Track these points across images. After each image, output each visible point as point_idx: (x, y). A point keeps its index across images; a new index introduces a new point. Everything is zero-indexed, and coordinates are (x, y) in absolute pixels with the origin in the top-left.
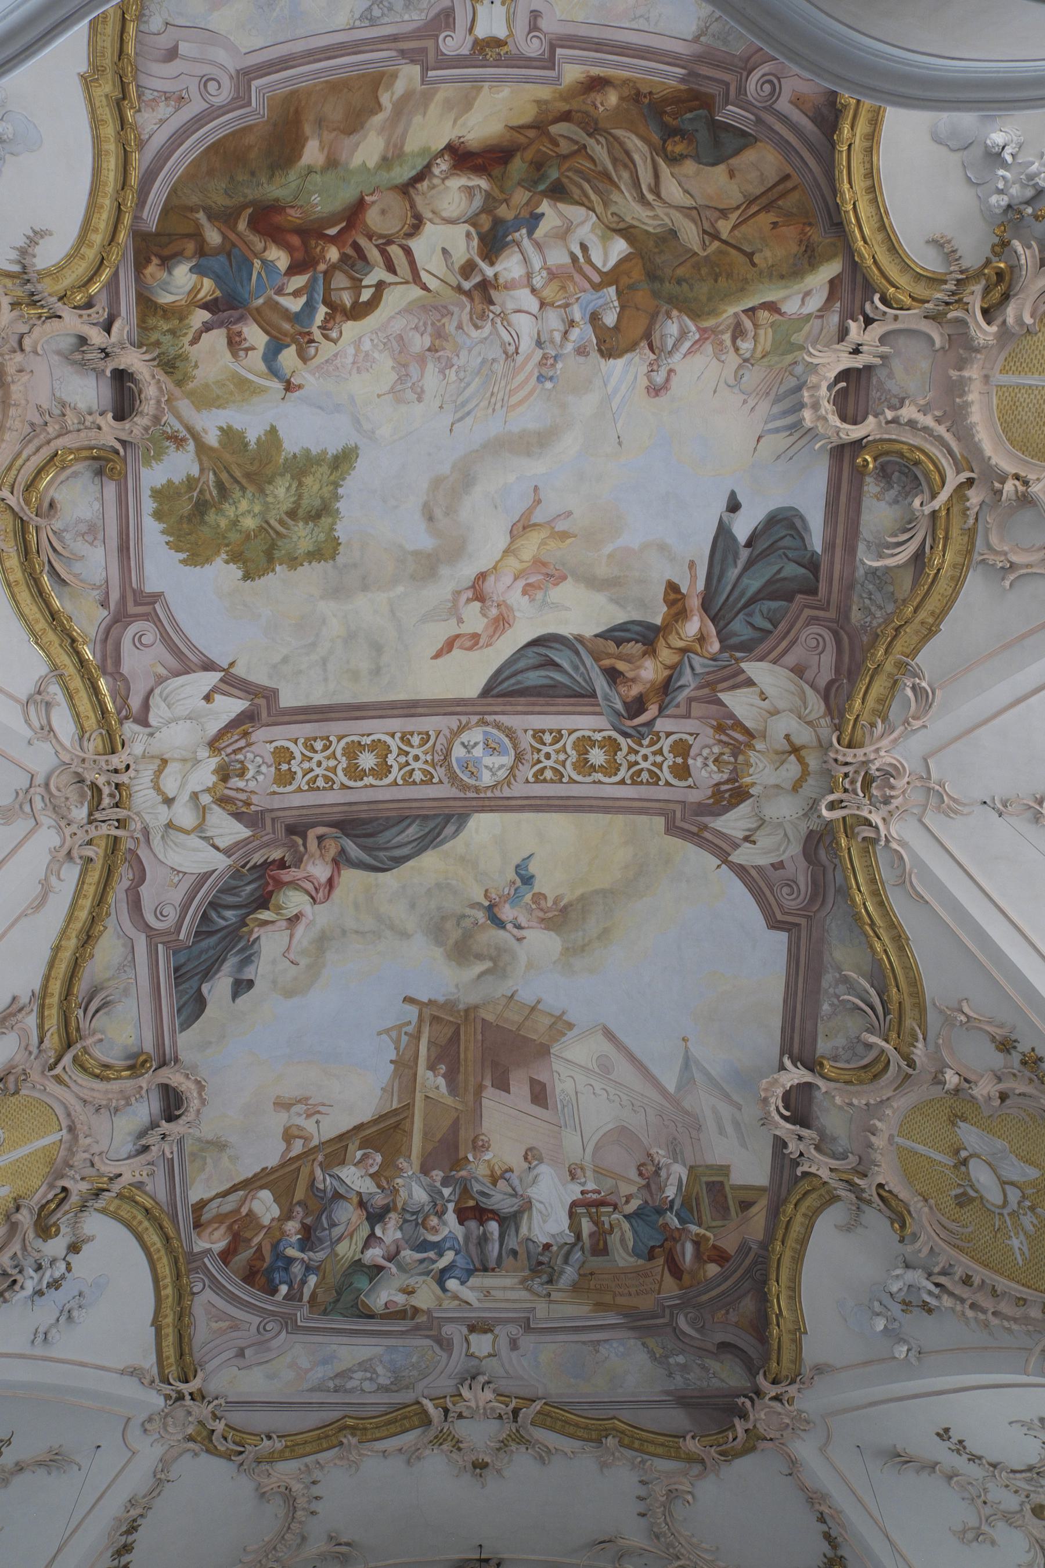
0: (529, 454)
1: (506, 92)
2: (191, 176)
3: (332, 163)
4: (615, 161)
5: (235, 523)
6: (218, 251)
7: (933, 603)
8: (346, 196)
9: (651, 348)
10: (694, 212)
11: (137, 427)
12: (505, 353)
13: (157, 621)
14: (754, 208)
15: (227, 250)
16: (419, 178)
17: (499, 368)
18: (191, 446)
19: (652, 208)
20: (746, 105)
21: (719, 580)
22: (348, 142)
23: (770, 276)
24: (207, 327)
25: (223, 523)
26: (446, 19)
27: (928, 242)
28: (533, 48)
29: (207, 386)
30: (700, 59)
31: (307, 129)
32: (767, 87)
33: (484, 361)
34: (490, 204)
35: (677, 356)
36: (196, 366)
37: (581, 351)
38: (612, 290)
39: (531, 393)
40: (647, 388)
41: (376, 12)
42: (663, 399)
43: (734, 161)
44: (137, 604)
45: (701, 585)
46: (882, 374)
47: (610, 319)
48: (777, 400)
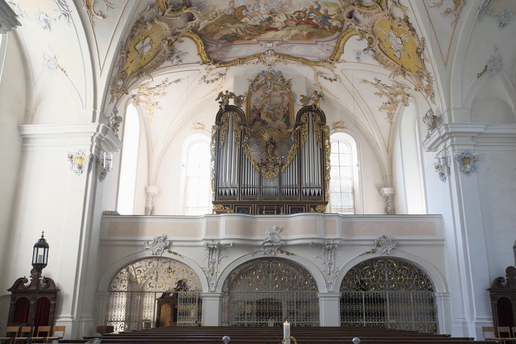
1: (267, 37)
2: (328, 36)
4: (245, 31)
6: (326, 25)
8: (299, 27)
9: (234, 8)
10: (228, 28)
11: (351, 8)
12: (267, 5)
14: (217, 32)
15: (324, 24)
16: (284, 27)
17: (268, 2)
19: (238, 27)
22: (298, 33)
23: (211, 24)
24: (331, 15)
26: (277, 45)
27: (184, 41)
28: (261, 43)
29: (334, 7)
30: (230, 46)
31: (306, 36)
32: (218, 46)
33: (272, 3)
34: (270, 24)
35: (228, 8)
36: (335, 10)
37: (250, 6)
38: (244, 15)
40: (234, 2)
41: (291, 47)
43: (222, 36)
46: (186, 19)
47: (244, 11)
48: (205, 7)
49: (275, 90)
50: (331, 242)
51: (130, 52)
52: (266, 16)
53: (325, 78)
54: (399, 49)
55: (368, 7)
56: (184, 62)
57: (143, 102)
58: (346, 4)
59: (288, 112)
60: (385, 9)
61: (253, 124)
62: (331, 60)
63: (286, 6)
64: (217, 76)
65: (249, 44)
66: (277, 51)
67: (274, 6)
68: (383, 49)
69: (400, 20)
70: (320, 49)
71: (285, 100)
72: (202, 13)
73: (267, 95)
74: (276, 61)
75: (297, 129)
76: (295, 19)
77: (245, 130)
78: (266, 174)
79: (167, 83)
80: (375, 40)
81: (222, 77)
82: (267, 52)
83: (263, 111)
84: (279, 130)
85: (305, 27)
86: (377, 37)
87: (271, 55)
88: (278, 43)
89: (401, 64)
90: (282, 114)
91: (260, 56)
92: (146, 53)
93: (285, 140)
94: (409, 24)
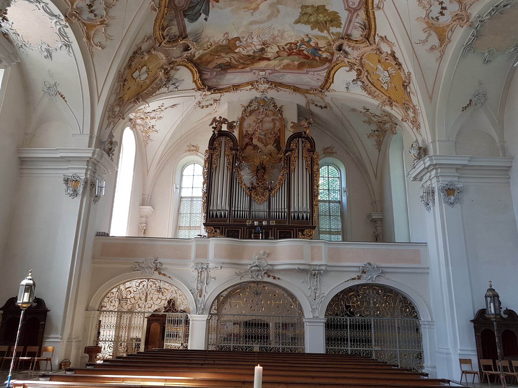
0: (254, 21)
1: (259, 66)
2: (318, 66)
3: (293, 61)
4: (239, 60)
5: (324, 16)
7: (158, 24)
8: (290, 57)
9: (229, 40)
10: (222, 57)
11: (340, 42)
13: (348, 5)
16: (276, 57)
18: (330, 32)
20: (215, 71)
21: (206, 6)
22: (290, 63)
24: (322, 48)
25: (327, 17)
26: (270, 74)
28: (254, 71)
29: (324, 40)
31: (297, 66)
34: (263, 54)
35: (223, 39)
36: (325, 43)
37: (243, 37)
38: (237, 45)
39: (253, 31)
41: (282, 75)
42: (225, 32)
43: (216, 65)
44: (351, 11)
45: (211, 4)
46: (182, 49)
47: (237, 42)
48: (201, 38)
49: (267, 115)
50: (317, 268)
51: (127, 80)
52: (259, 47)
53: (316, 105)
54: (387, 81)
55: (356, 41)
56: (179, 88)
57: (139, 125)
58: (335, 37)
59: (279, 137)
60: (373, 44)
61: (245, 148)
62: (321, 89)
63: (278, 38)
64: (212, 102)
65: (243, 72)
66: (269, 79)
67: (267, 38)
68: (371, 81)
69: (387, 55)
70: (311, 79)
71: (276, 126)
72: (197, 43)
73: (259, 121)
74: (269, 88)
75: (287, 154)
76: (287, 50)
77: (236, 155)
78: (256, 198)
79: (163, 108)
80: (363, 72)
81: (217, 103)
82: (260, 80)
83: (255, 135)
84: (270, 155)
85: (296, 57)
86: (365, 69)
87: (264, 83)
88: (270, 71)
89: (388, 95)
90: (274, 139)
91: (253, 84)
92: (142, 81)
93: (275, 164)
94: (395, 58)
